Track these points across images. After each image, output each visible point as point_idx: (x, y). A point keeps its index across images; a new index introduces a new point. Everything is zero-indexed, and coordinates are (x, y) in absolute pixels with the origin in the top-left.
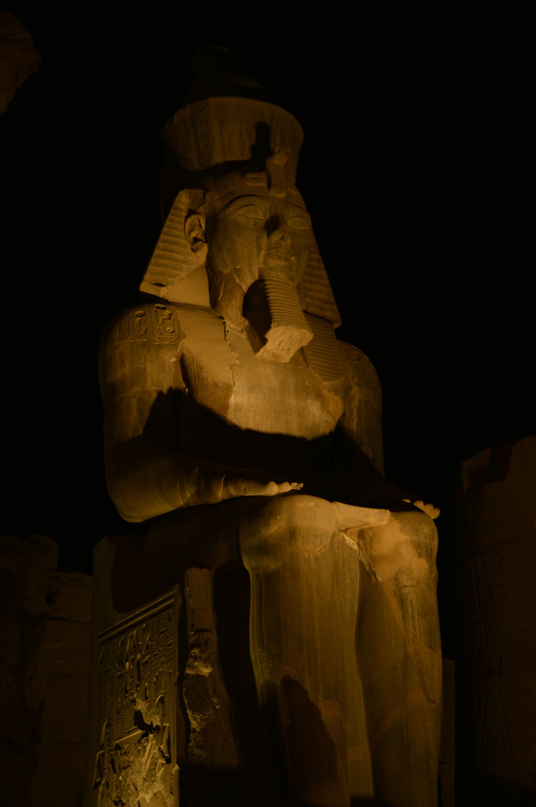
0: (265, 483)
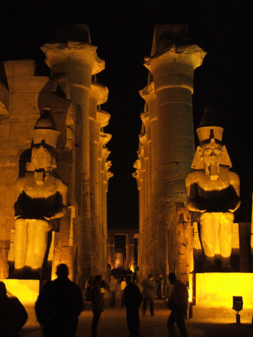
0: (201, 210)
